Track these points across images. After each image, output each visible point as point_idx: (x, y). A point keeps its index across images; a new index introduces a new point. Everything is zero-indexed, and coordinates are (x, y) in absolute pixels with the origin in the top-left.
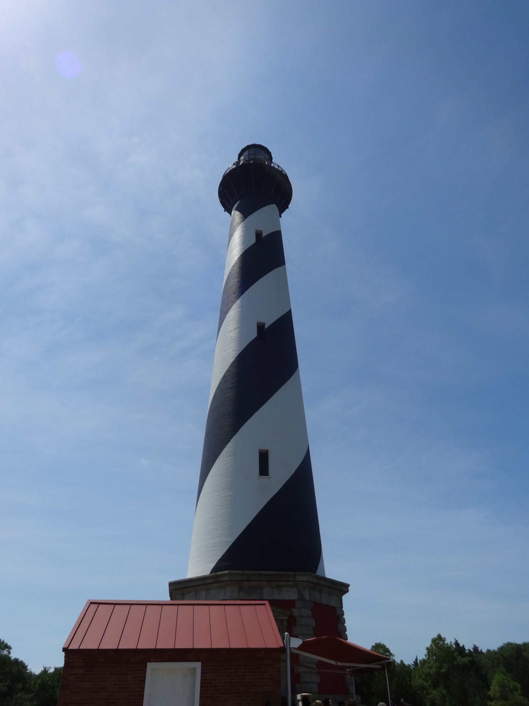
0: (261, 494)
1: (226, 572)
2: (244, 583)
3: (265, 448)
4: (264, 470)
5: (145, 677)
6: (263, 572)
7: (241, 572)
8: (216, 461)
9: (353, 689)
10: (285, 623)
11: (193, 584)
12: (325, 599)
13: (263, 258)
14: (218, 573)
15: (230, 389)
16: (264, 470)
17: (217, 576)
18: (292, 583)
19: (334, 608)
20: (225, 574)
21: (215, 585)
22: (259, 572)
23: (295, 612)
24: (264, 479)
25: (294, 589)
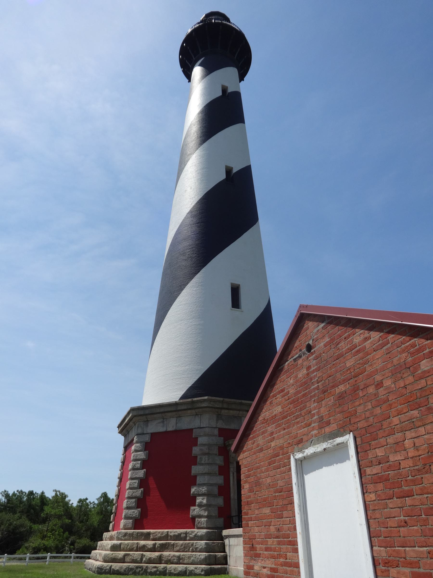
0: (233, 327)
1: (206, 398)
2: (224, 412)
3: (237, 283)
4: (236, 302)
6: (243, 401)
7: (221, 399)
8: (183, 291)
11: (162, 410)
13: (222, 114)
14: (195, 399)
15: (198, 223)
16: (236, 302)
17: (193, 402)
20: (204, 400)
21: (189, 411)
22: (240, 401)
24: (236, 312)
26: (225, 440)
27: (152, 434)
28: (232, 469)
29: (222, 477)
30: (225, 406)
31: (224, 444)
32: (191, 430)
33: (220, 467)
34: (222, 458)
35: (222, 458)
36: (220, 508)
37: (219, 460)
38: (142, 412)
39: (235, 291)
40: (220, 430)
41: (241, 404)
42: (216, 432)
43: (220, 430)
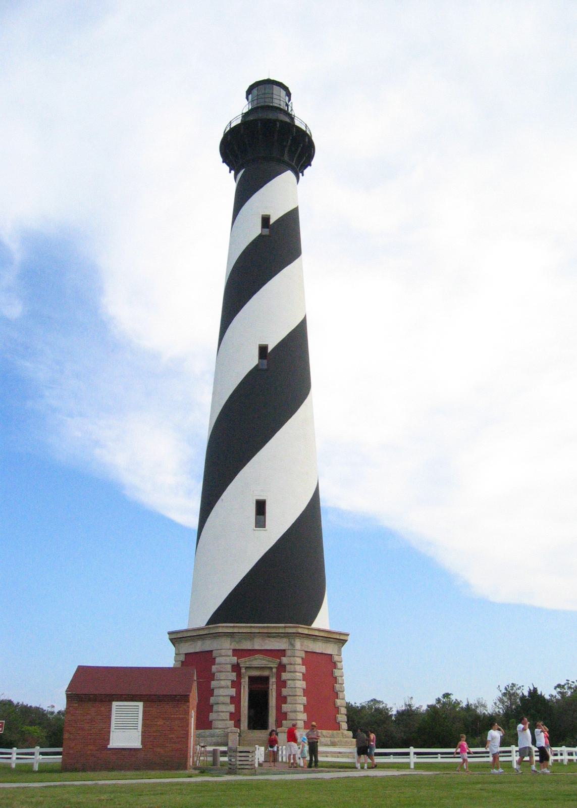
5: (111, 709)
9: (344, 726)
10: (274, 670)
12: (319, 647)
14: (210, 626)
18: (282, 635)
19: (331, 655)
23: (285, 660)
24: (260, 532)
25: (285, 640)
26: (238, 659)
27: (186, 654)
28: (243, 683)
29: (234, 689)
30: (236, 630)
31: (237, 662)
32: (212, 651)
33: (233, 682)
34: (234, 674)
35: (234, 674)
36: (231, 713)
37: (233, 676)
38: (174, 636)
39: (261, 507)
40: (234, 650)
41: (251, 627)
42: (230, 653)
43: (234, 650)
